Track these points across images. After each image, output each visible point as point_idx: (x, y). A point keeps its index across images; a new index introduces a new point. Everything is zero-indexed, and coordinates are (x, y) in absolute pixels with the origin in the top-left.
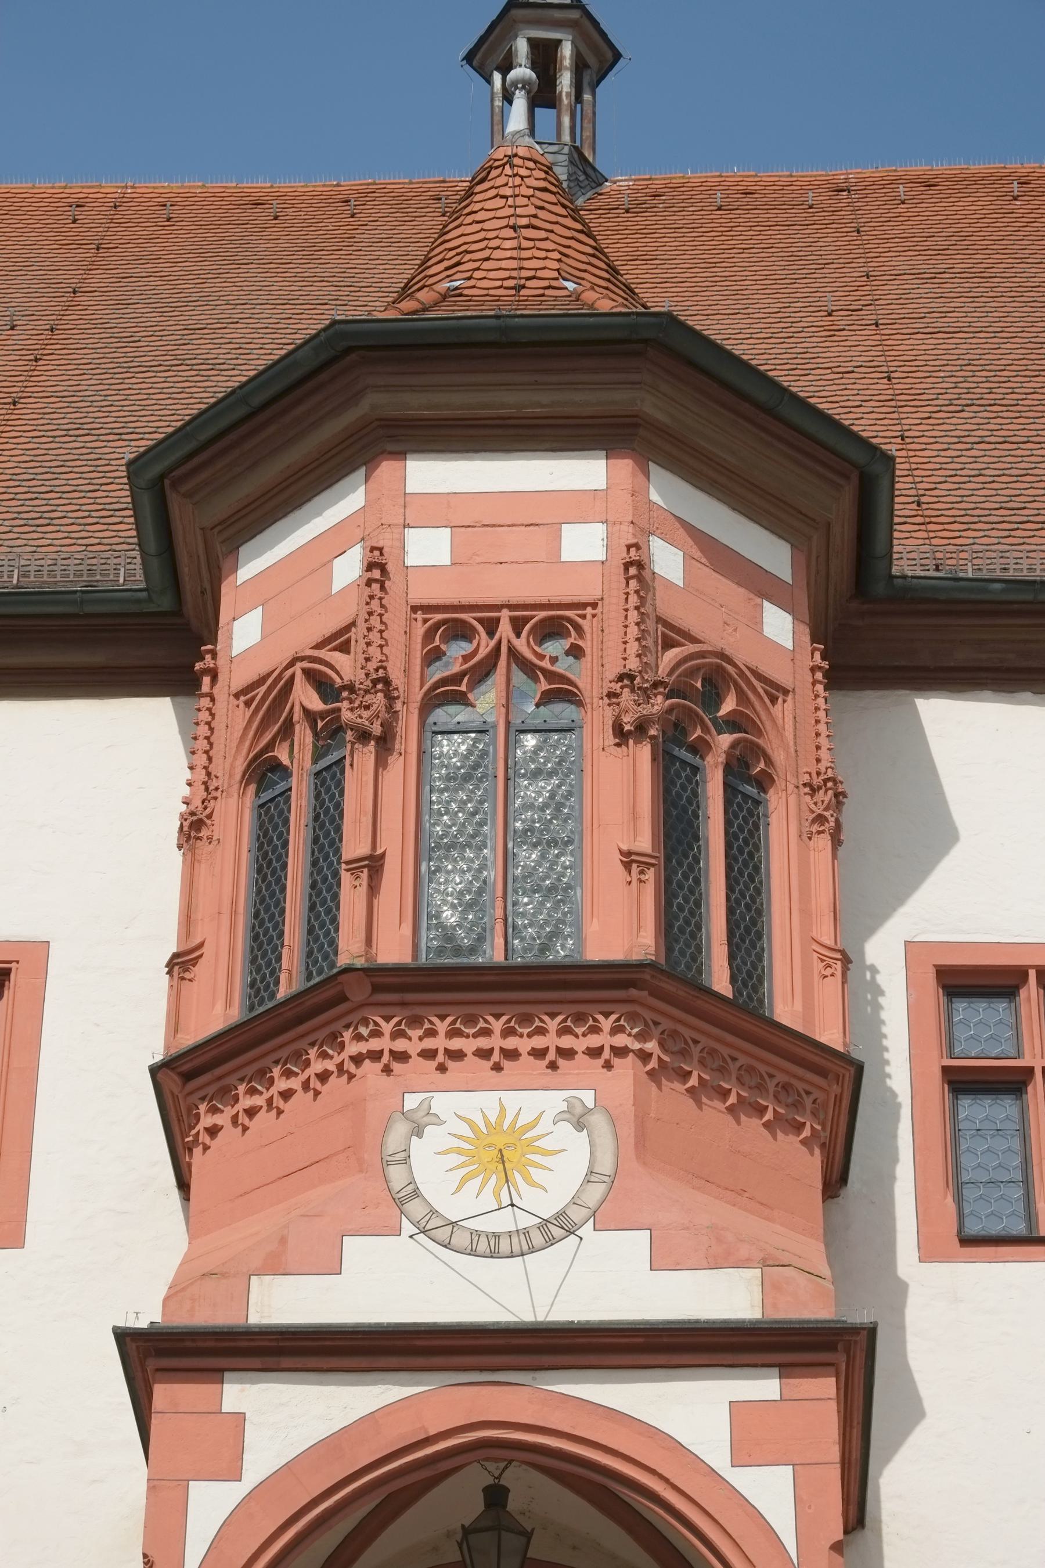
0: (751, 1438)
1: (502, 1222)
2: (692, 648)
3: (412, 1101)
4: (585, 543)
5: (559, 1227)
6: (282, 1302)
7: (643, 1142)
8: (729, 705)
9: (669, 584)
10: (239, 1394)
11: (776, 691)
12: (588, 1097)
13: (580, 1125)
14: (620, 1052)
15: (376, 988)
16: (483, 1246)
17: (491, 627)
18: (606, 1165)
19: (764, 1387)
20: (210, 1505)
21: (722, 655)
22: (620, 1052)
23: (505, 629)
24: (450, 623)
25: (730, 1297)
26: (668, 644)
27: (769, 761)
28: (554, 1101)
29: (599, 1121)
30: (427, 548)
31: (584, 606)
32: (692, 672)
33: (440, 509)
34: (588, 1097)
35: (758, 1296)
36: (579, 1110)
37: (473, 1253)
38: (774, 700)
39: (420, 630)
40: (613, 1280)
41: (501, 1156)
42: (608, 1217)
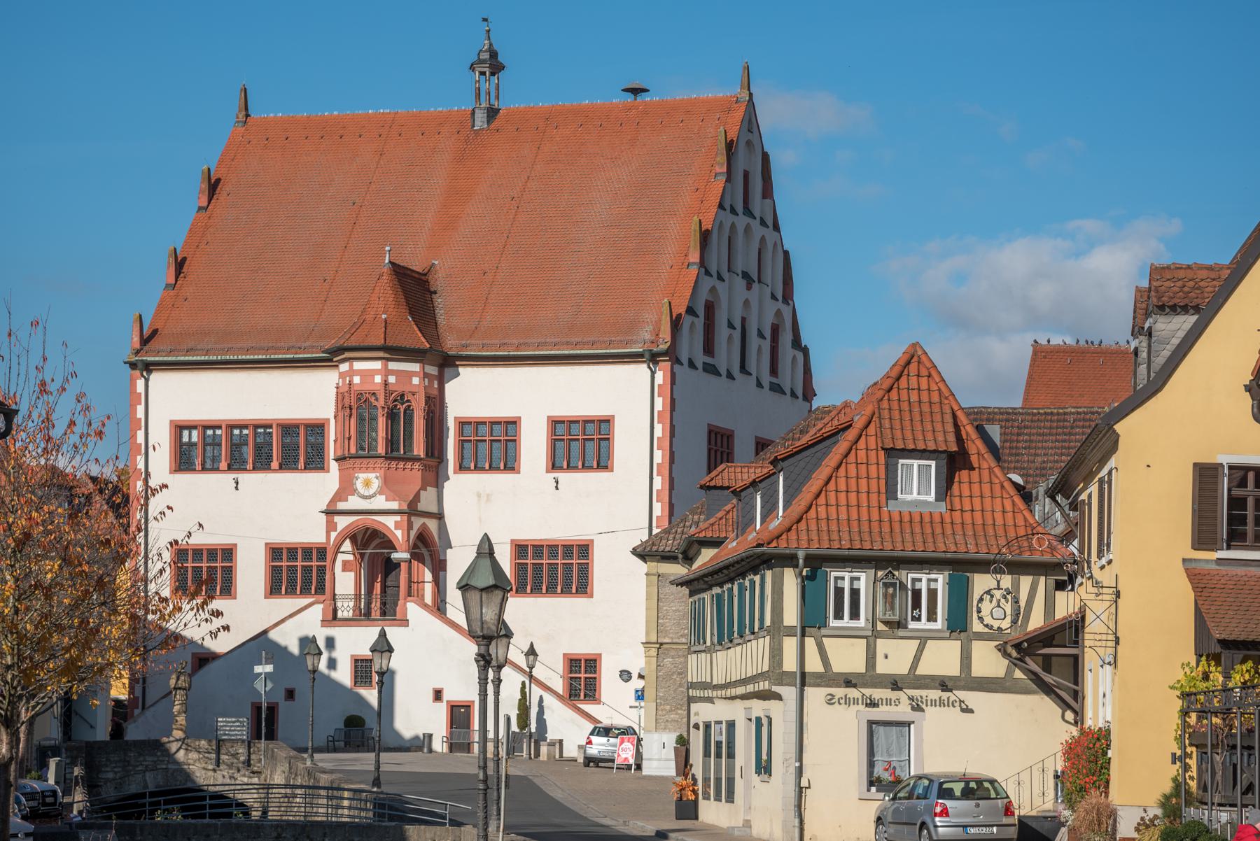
0: (397, 525)
1: (366, 494)
4: (378, 379)
5: (370, 497)
6: (341, 506)
10: (337, 519)
19: (398, 518)
20: (333, 535)
24: (360, 395)
25: (394, 505)
30: (357, 380)
33: (359, 372)
40: (380, 503)
41: (367, 484)
42: (381, 493)
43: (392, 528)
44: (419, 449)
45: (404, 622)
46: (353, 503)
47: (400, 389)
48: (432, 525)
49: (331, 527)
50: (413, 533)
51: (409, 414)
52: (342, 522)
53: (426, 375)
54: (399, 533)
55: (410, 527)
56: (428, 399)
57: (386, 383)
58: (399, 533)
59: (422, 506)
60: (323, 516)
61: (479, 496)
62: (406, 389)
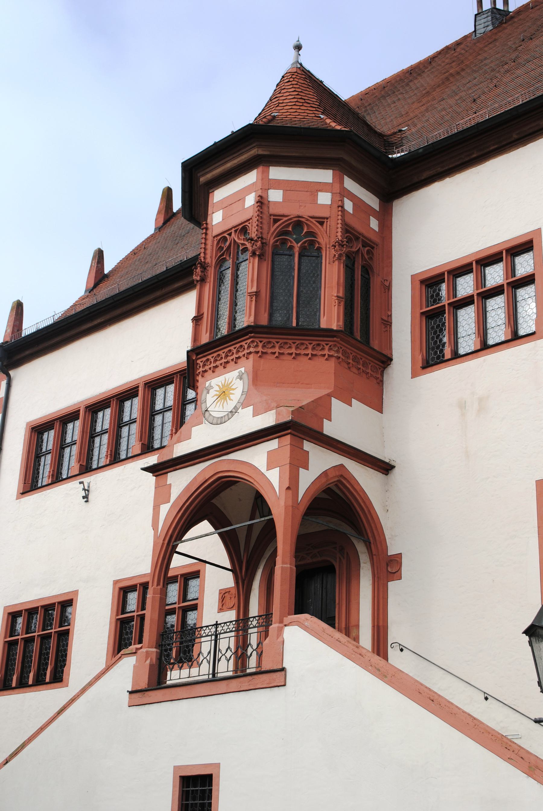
2: (286, 219)
3: (207, 384)
4: (250, 200)
7: (256, 379)
8: (305, 230)
9: (275, 203)
11: (321, 221)
12: (243, 370)
13: (241, 379)
14: (250, 353)
15: (197, 354)
16: (219, 422)
17: (230, 234)
18: (246, 390)
19: (273, 444)
20: (165, 509)
21: (299, 217)
22: (250, 353)
23: (233, 234)
25: (268, 420)
26: (276, 221)
27: (319, 243)
28: (236, 373)
29: (245, 376)
31: (249, 220)
32: (288, 225)
34: (243, 370)
35: (275, 418)
36: (241, 374)
37: (217, 424)
38: (322, 223)
39: (215, 243)
41: (224, 394)
42: (244, 404)
43: (263, 469)
44: (331, 317)
45: (274, 675)
46: (201, 437)
47: (293, 211)
48: (364, 477)
49: (161, 494)
50: (307, 479)
51: (311, 251)
52: (181, 481)
53: (345, 193)
54: (274, 477)
55: (299, 461)
56: (350, 234)
57: (261, 202)
58: (274, 477)
59: (329, 429)
60: (150, 478)
61: (462, 406)
62: (306, 212)
